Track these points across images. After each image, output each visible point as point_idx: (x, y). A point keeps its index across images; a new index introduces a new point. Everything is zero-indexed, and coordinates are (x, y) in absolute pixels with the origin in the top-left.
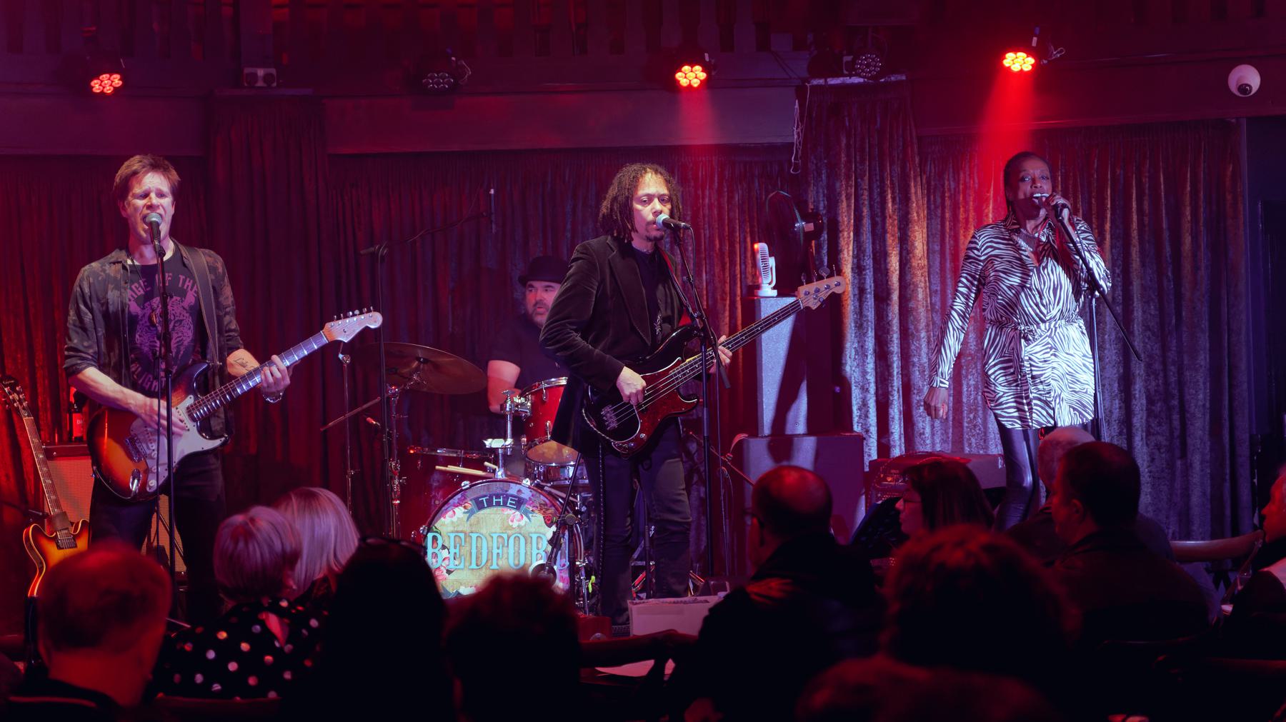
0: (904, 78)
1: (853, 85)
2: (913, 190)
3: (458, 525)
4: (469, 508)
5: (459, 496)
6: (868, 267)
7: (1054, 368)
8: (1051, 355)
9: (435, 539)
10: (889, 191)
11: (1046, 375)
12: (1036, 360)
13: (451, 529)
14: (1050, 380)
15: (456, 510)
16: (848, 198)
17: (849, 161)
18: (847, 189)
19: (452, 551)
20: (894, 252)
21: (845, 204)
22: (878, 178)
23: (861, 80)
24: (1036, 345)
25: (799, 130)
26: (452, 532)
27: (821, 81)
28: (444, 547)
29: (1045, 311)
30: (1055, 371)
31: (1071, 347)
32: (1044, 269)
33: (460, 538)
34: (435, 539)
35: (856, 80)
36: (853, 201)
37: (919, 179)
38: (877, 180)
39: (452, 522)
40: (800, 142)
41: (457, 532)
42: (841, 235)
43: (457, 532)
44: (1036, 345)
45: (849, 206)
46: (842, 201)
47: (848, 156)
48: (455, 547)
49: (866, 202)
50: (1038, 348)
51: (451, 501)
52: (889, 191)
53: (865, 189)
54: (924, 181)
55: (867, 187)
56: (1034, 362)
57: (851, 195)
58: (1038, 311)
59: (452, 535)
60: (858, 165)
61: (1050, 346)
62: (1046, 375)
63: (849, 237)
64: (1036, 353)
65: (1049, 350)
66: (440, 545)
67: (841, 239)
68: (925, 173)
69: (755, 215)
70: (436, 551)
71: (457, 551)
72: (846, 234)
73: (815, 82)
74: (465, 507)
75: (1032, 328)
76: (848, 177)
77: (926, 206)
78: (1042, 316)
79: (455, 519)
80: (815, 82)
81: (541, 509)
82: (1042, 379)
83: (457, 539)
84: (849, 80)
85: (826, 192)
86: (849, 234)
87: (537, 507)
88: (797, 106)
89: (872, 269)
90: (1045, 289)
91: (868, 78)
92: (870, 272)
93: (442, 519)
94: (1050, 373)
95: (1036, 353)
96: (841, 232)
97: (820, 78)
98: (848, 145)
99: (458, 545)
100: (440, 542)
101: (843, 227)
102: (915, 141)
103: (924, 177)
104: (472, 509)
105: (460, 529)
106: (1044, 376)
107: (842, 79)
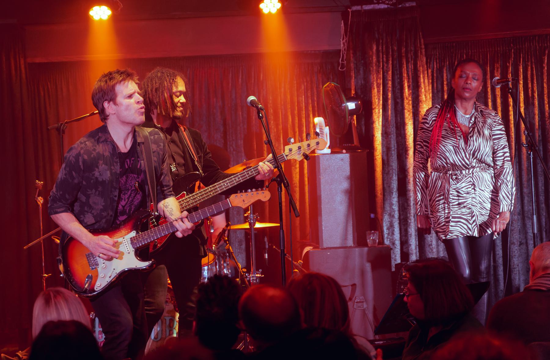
0: (414, 4)
1: (380, 10)
2: (422, 80)
6: (392, 133)
7: (474, 198)
8: (472, 189)
10: (406, 81)
11: (468, 202)
12: (462, 192)
14: (470, 205)
16: (378, 87)
17: (378, 61)
18: (377, 80)
20: (410, 122)
21: (376, 90)
22: (398, 72)
23: (386, 6)
24: (463, 182)
25: (344, 41)
27: (358, 8)
29: (468, 163)
30: (474, 200)
31: (483, 186)
32: (471, 137)
35: (383, 6)
36: (381, 88)
37: (426, 72)
38: (397, 74)
40: (345, 49)
42: (374, 111)
44: (463, 182)
45: (379, 92)
46: (374, 89)
47: (378, 57)
49: (390, 89)
50: (464, 185)
52: (406, 81)
53: (389, 80)
54: (430, 74)
55: (390, 79)
56: (461, 194)
57: (380, 84)
58: (464, 163)
60: (385, 64)
61: (471, 183)
62: (468, 202)
63: (379, 113)
64: (462, 188)
65: (470, 186)
67: (374, 114)
68: (430, 68)
69: (315, 99)
72: (377, 110)
73: (355, 8)
75: (457, 172)
76: (378, 72)
77: (431, 91)
78: (467, 166)
80: (355, 8)
81: (172, 300)
82: (465, 205)
84: (377, 7)
85: (363, 82)
86: (379, 111)
87: (169, 299)
88: (342, 25)
89: (395, 134)
90: (469, 150)
91: (391, 5)
92: (394, 136)
94: (471, 201)
95: (462, 188)
96: (373, 109)
97: (358, 5)
98: (378, 50)
101: (375, 106)
102: (423, 47)
103: (430, 71)
106: (466, 203)
107: (372, 6)
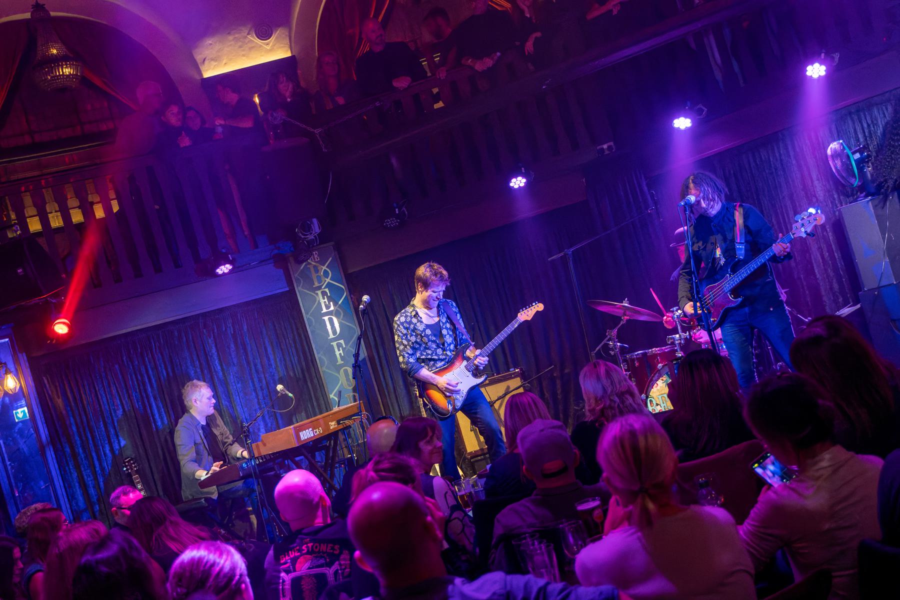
3: (661, 391)
4: (665, 379)
5: (657, 375)
9: (651, 401)
13: (658, 394)
15: (658, 382)
19: (662, 405)
26: (659, 395)
28: (657, 405)
33: (665, 397)
34: (651, 401)
39: (658, 390)
41: (662, 394)
43: (662, 394)
48: (663, 403)
51: (654, 379)
59: (660, 397)
66: (655, 404)
70: (653, 408)
71: (665, 405)
74: (662, 380)
79: (658, 388)
83: (663, 399)
93: (652, 390)
99: (665, 402)
100: (654, 402)
104: (666, 380)
105: (663, 392)
